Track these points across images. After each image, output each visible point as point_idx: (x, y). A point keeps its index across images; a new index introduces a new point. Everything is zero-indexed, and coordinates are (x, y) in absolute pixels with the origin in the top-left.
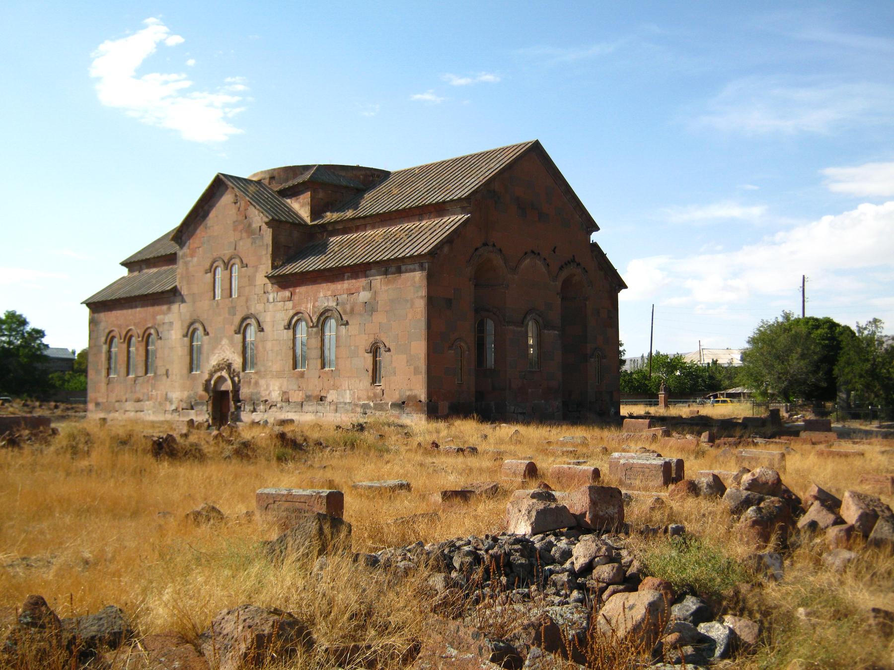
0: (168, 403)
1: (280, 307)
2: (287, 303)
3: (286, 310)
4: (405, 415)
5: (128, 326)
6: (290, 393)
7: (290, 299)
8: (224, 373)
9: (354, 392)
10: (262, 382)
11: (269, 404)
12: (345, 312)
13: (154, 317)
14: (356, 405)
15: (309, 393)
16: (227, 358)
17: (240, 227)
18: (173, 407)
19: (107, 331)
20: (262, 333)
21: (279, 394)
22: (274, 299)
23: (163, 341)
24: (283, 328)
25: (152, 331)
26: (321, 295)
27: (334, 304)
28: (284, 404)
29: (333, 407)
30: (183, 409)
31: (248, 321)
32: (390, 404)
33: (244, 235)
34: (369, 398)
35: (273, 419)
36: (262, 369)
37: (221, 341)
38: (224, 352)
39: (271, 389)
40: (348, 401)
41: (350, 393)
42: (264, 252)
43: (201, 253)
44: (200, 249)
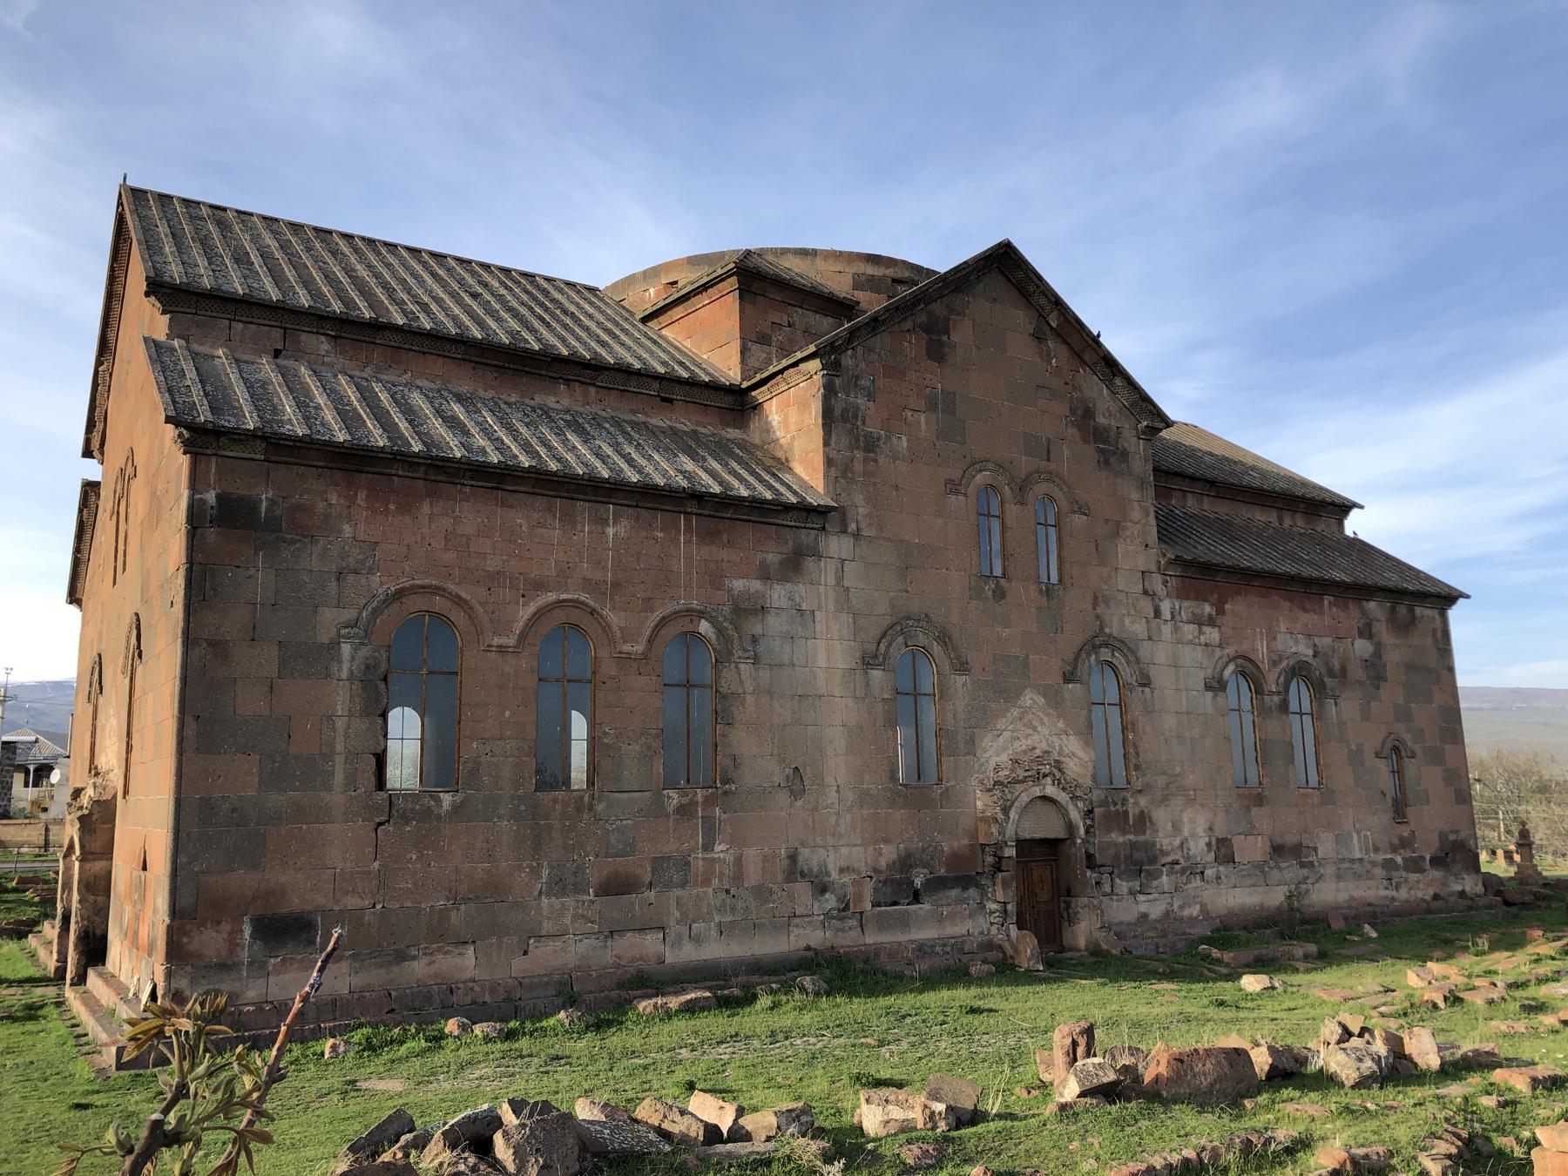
0: (803, 889)
1: (1190, 637)
2: (1207, 629)
3: (1206, 645)
4: (1452, 878)
5: (540, 586)
6: (1237, 841)
7: (1211, 622)
8: (1050, 790)
9: (1366, 837)
10: (1161, 816)
11: (1183, 871)
12: (1331, 674)
13: (715, 579)
14: (1374, 864)
15: (1279, 841)
16: (1044, 745)
17: (1064, 409)
18: (830, 901)
19: (381, 585)
20: (1147, 690)
21: (1209, 845)
22: (1173, 617)
23: (765, 674)
24: (1203, 685)
25: (704, 627)
26: (1283, 629)
27: (1310, 652)
28: (1221, 868)
29: (1329, 870)
30: (875, 904)
31: (1105, 654)
32: (1428, 858)
33: (1073, 432)
34: (1394, 849)
35: (1198, 907)
36: (1161, 781)
37: (1018, 696)
38: (1035, 729)
39: (1186, 834)
40: (1358, 855)
41: (1359, 840)
42: (1135, 495)
43: (923, 427)
44: (923, 418)
